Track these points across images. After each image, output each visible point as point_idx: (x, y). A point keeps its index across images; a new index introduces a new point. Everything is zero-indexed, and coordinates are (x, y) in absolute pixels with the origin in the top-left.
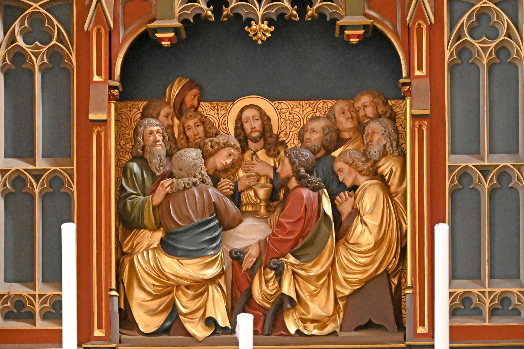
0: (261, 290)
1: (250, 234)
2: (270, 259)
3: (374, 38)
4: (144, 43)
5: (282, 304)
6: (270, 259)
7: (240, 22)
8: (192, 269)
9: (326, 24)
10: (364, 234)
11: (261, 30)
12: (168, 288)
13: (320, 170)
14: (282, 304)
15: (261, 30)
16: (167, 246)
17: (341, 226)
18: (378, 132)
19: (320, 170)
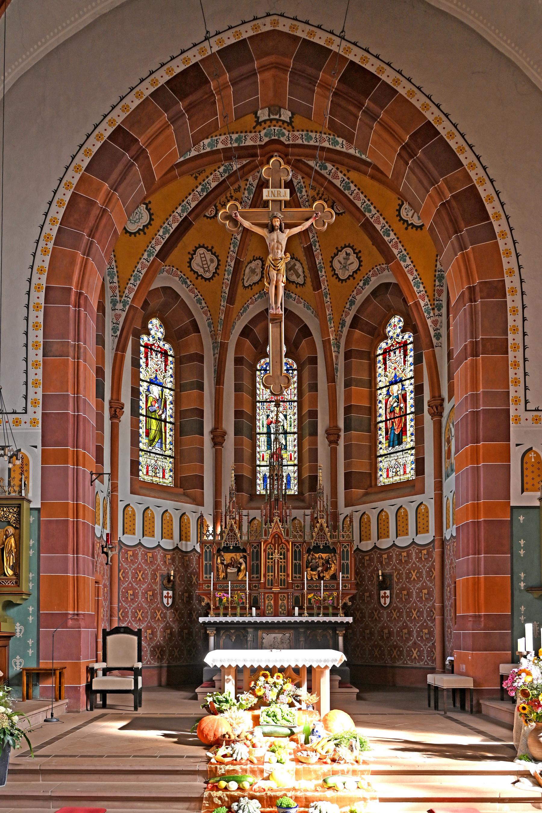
0: (321, 575)
1: (320, 569)
2: (322, 572)
3: (334, 548)
4: (309, 548)
5: (324, 577)
6: (322, 572)
7: (319, 546)
8: (314, 573)
9: (329, 547)
10: (332, 569)
11: (322, 547)
12: (311, 575)
13: (327, 562)
14: (324, 577)
15: (322, 547)
16: (312, 570)
17: (330, 568)
18: (334, 558)
19: (327, 562)
